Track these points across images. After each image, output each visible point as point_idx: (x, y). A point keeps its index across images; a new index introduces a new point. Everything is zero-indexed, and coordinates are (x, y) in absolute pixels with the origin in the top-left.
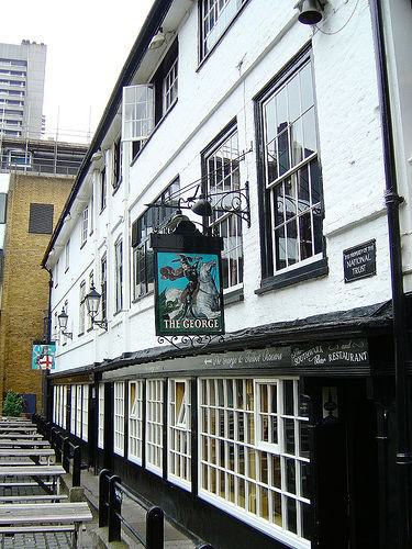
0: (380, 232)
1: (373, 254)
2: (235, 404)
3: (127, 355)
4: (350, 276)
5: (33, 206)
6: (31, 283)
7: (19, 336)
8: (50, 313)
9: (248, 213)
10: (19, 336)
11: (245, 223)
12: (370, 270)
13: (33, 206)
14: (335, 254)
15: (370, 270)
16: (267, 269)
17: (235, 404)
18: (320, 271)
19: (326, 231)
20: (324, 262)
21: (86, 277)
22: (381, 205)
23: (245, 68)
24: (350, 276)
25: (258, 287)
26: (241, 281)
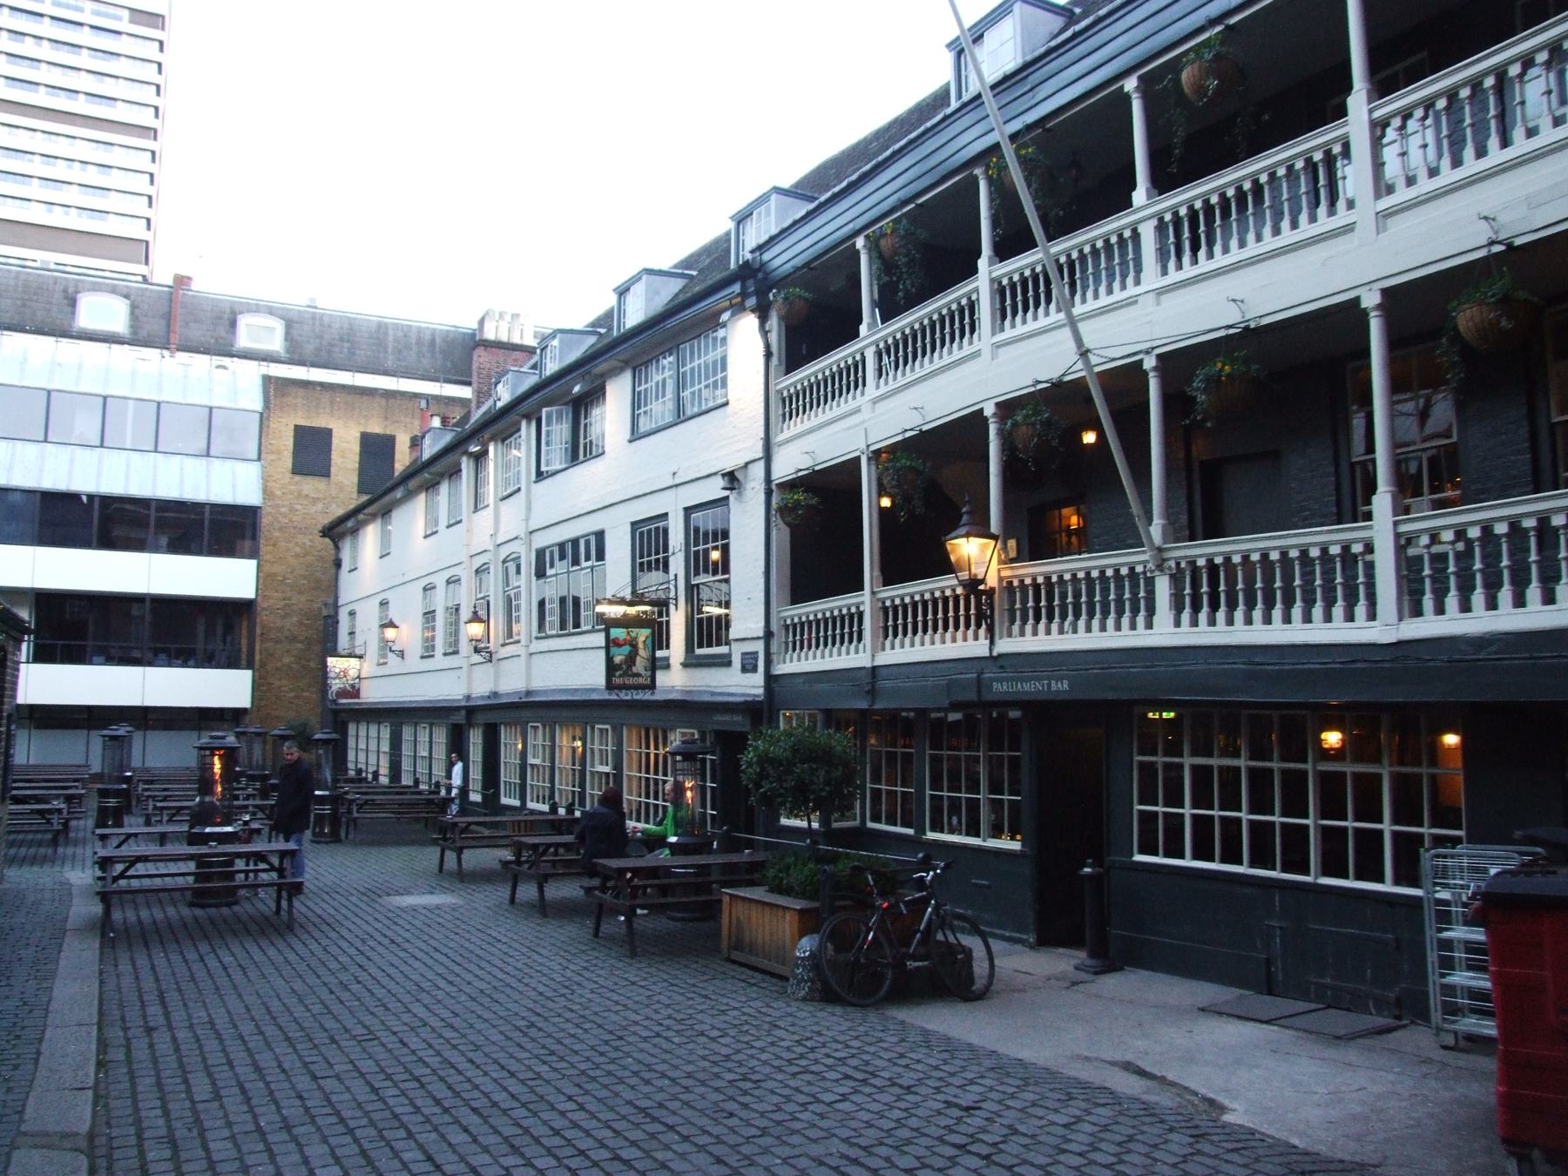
0: (759, 647)
1: (756, 659)
2: (652, 747)
3: (528, 693)
4: (744, 670)
5: (299, 430)
6: (297, 556)
7: (278, 641)
8: (336, 607)
9: (676, 599)
10: (278, 641)
11: (672, 607)
12: (754, 669)
13: (299, 430)
14: (737, 651)
15: (754, 669)
16: (689, 648)
17: (652, 747)
18: (725, 662)
19: (732, 636)
20: (729, 655)
21: (440, 580)
22: (761, 634)
23: (678, 481)
24: (744, 670)
25: (682, 660)
26: (668, 647)
